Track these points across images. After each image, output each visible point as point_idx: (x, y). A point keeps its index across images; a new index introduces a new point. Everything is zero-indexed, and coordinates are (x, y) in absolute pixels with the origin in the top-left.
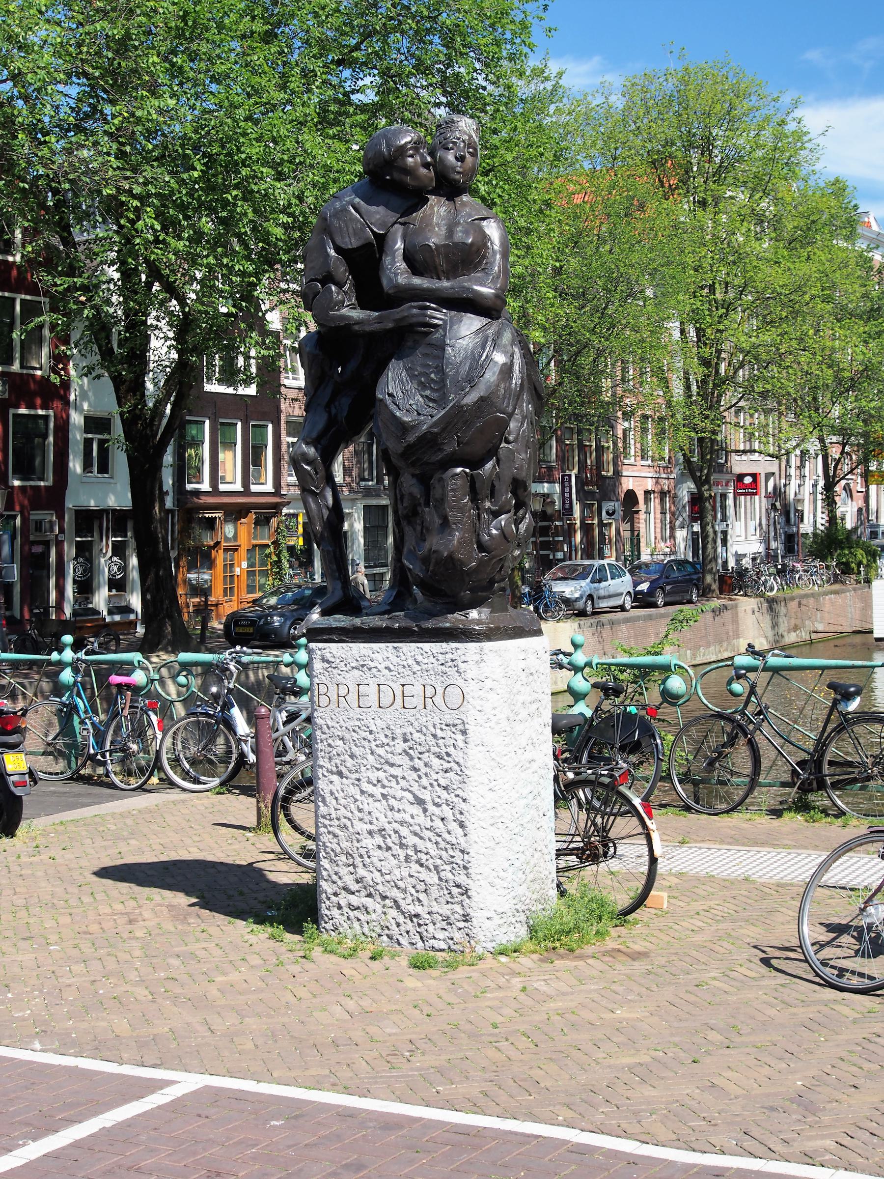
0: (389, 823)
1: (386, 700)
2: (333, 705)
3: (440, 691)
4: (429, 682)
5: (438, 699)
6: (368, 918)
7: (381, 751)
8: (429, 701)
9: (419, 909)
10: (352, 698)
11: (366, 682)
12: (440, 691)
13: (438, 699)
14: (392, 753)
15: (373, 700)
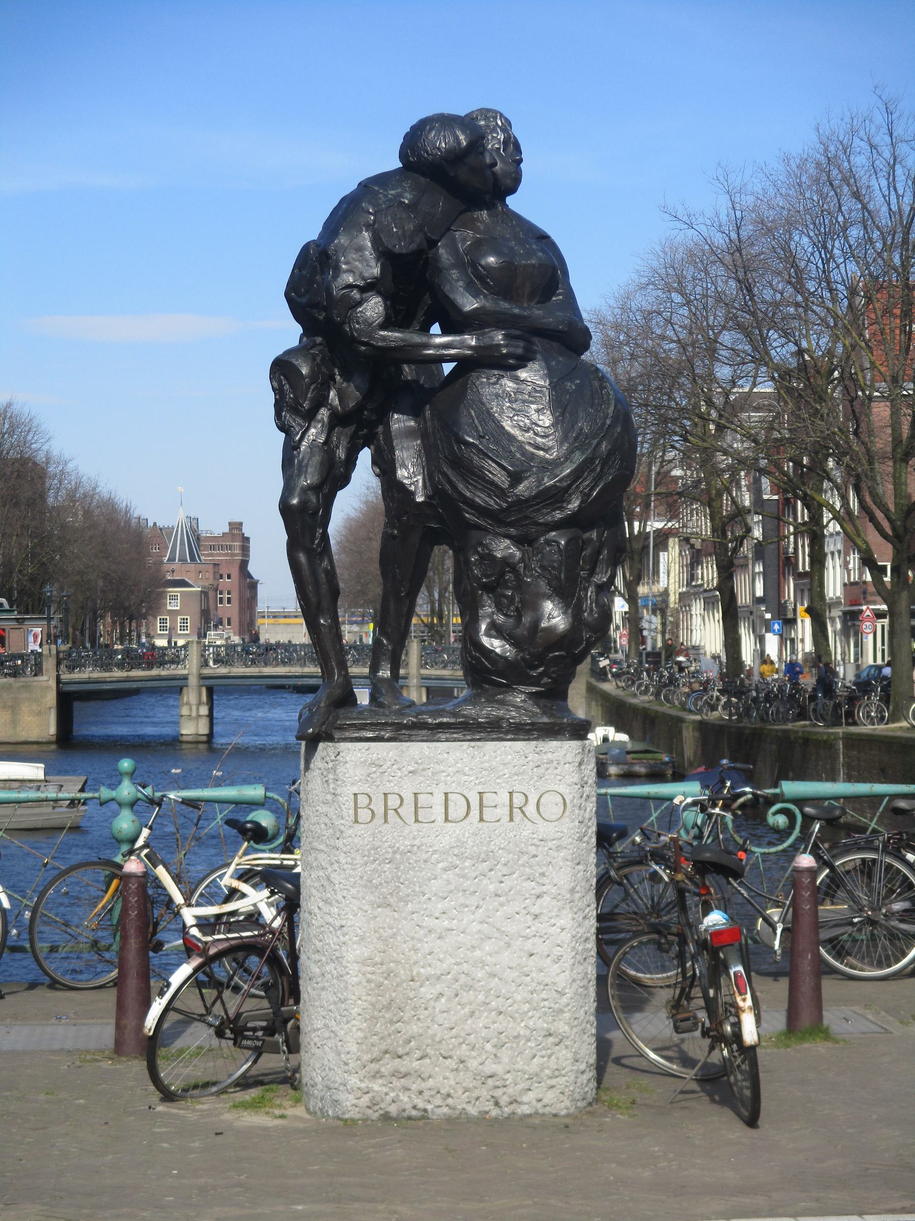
0: (457, 964)
1: (457, 809)
2: (379, 820)
3: (533, 800)
4: (517, 788)
5: (531, 809)
6: (424, 1085)
7: (450, 875)
8: (516, 811)
9: (498, 1069)
10: (407, 811)
11: (429, 790)
12: (533, 800)
13: (531, 809)
14: (464, 876)
15: (439, 810)
